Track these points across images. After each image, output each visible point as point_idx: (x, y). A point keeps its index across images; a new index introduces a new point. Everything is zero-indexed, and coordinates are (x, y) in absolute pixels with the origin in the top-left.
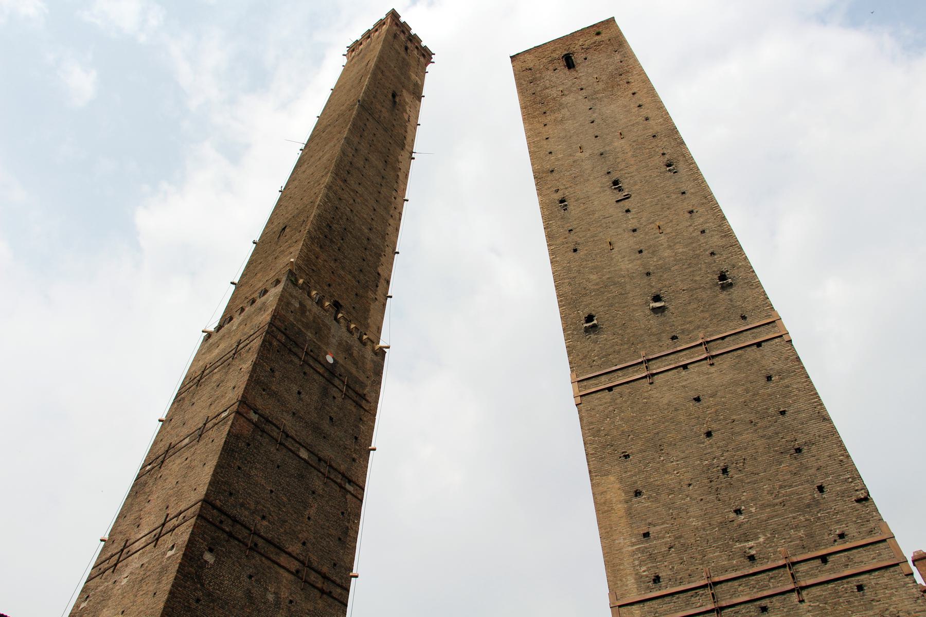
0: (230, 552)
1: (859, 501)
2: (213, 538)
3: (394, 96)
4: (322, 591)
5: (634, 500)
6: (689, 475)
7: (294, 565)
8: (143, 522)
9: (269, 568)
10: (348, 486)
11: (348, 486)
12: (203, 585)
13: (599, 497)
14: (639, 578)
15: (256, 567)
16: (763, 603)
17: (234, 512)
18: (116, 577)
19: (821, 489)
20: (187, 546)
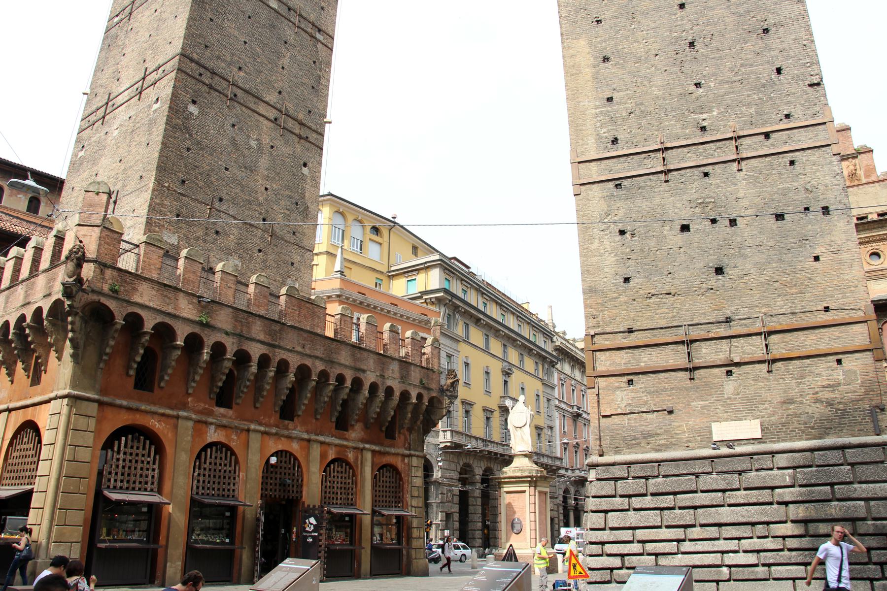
0: (212, 104)
1: (811, 85)
2: (194, 91)
4: (300, 137)
5: (603, 65)
6: (657, 46)
7: (272, 114)
8: (123, 75)
9: (250, 116)
10: (318, 36)
11: (318, 36)
12: (191, 135)
13: (568, 60)
14: (599, 138)
15: (238, 117)
16: (706, 169)
17: (210, 65)
18: (106, 128)
19: (779, 71)
20: (171, 99)
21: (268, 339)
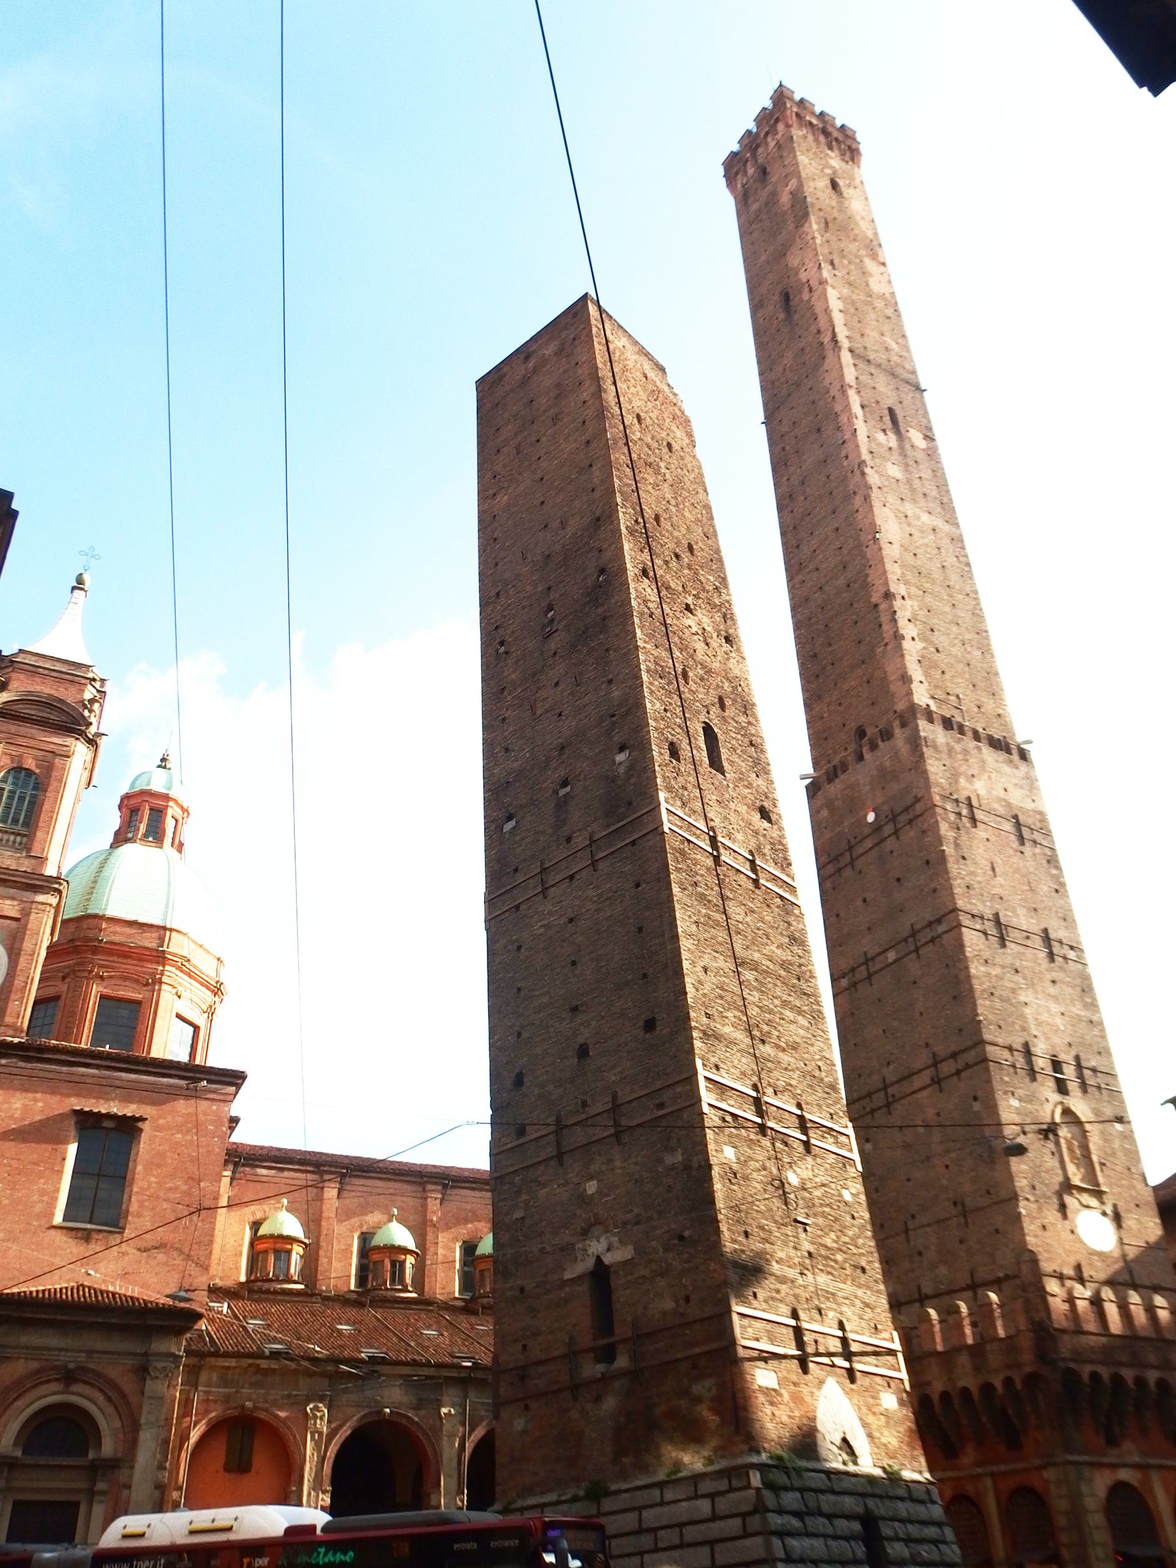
3: (786, 298)
4: (958, 1073)
10: (941, 929)
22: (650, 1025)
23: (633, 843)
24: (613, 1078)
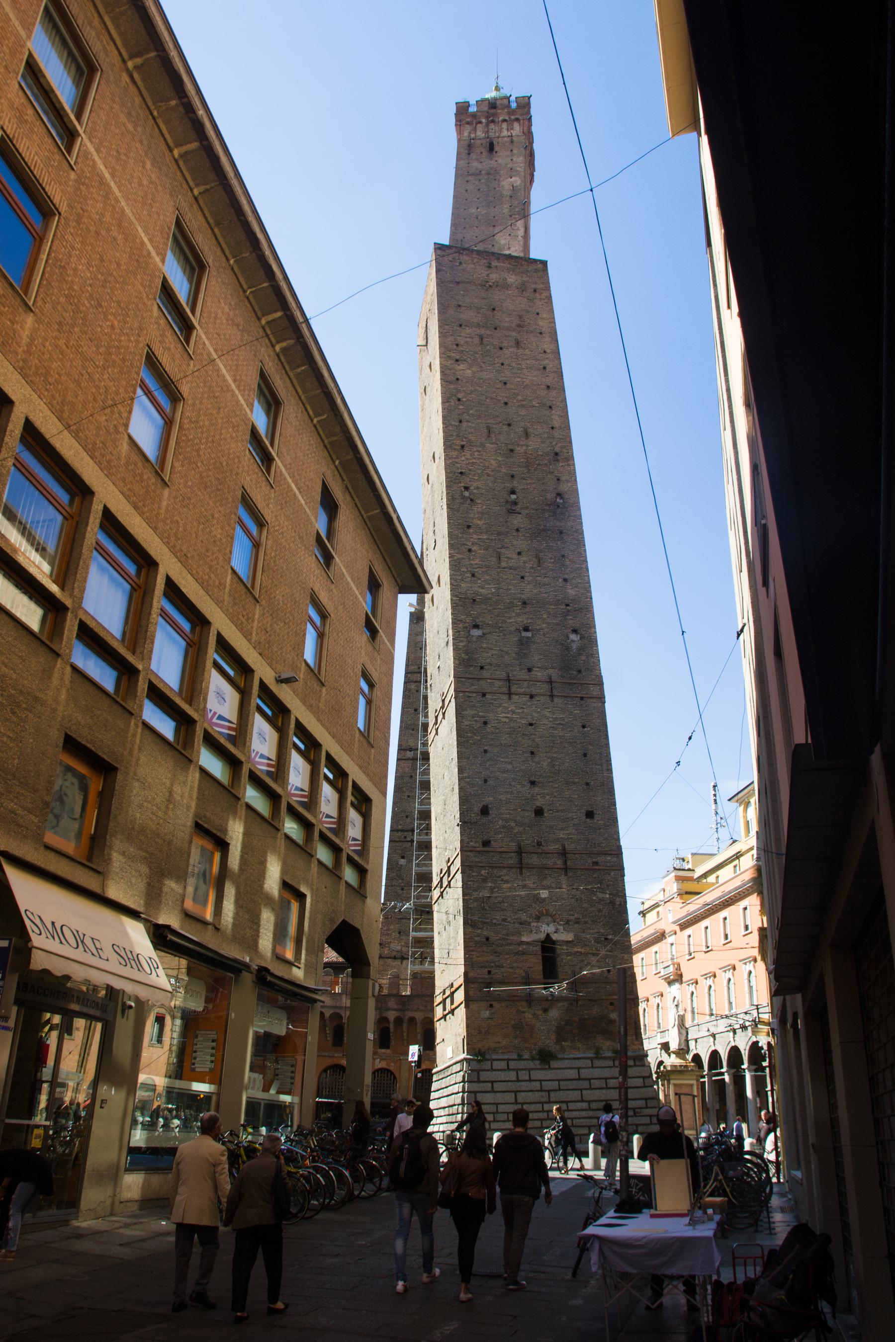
21: (400, 1007)
22: (590, 815)
23: (582, 698)
24: (562, 836)
